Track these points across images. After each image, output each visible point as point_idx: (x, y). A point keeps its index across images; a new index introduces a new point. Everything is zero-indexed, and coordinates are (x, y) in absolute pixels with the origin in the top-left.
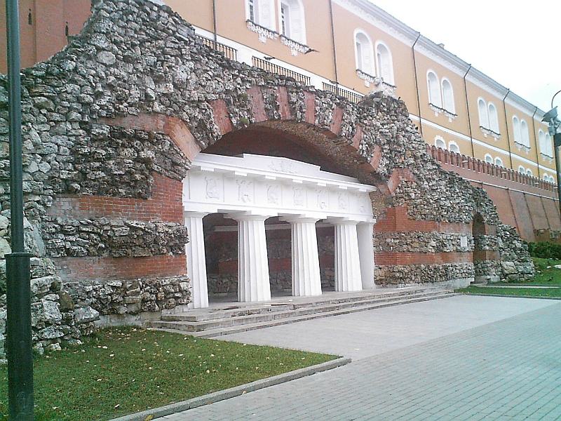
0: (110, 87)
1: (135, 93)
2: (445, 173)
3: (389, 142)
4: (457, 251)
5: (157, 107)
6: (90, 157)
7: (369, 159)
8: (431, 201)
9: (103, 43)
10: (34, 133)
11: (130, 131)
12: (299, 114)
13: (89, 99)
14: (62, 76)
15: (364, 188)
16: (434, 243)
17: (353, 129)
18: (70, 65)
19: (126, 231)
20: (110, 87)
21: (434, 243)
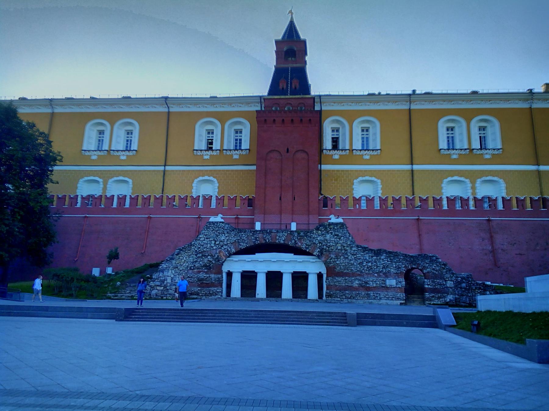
0: (203, 246)
1: (209, 245)
2: (372, 250)
3: (320, 243)
4: (383, 287)
5: (214, 248)
6: (196, 261)
7: (308, 250)
8: (355, 264)
9: (201, 236)
10: (185, 259)
11: (207, 254)
12: (267, 240)
13: (196, 249)
14: (191, 245)
15: (314, 260)
16: (357, 282)
17: (295, 241)
18: (193, 243)
19: (203, 277)
20: (203, 246)
21: (357, 282)
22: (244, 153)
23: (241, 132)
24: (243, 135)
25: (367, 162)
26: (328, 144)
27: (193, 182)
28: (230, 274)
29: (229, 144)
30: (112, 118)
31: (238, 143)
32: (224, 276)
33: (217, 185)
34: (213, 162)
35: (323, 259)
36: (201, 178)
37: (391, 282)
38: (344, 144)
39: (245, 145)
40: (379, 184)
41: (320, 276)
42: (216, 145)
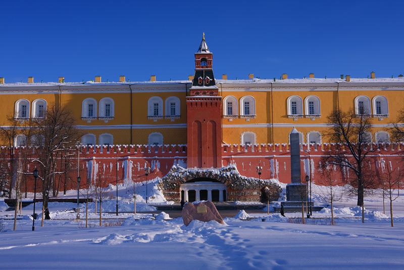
22: (177, 118)
23: (174, 104)
24: (176, 106)
25: (248, 123)
26: (225, 113)
27: (148, 136)
28: (183, 192)
29: (168, 112)
30: (98, 97)
31: (173, 110)
32: (180, 192)
33: (163, 137)
34: (160, 122)
35: (226, 184)
36: (153, 133)
37: (255, 193)
38: (235, 112)
39: (178, 112)
40: (255, 136)
41: (224, 191)
42: (161, 113)
